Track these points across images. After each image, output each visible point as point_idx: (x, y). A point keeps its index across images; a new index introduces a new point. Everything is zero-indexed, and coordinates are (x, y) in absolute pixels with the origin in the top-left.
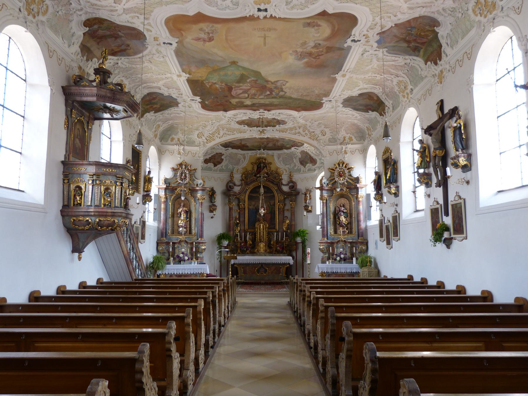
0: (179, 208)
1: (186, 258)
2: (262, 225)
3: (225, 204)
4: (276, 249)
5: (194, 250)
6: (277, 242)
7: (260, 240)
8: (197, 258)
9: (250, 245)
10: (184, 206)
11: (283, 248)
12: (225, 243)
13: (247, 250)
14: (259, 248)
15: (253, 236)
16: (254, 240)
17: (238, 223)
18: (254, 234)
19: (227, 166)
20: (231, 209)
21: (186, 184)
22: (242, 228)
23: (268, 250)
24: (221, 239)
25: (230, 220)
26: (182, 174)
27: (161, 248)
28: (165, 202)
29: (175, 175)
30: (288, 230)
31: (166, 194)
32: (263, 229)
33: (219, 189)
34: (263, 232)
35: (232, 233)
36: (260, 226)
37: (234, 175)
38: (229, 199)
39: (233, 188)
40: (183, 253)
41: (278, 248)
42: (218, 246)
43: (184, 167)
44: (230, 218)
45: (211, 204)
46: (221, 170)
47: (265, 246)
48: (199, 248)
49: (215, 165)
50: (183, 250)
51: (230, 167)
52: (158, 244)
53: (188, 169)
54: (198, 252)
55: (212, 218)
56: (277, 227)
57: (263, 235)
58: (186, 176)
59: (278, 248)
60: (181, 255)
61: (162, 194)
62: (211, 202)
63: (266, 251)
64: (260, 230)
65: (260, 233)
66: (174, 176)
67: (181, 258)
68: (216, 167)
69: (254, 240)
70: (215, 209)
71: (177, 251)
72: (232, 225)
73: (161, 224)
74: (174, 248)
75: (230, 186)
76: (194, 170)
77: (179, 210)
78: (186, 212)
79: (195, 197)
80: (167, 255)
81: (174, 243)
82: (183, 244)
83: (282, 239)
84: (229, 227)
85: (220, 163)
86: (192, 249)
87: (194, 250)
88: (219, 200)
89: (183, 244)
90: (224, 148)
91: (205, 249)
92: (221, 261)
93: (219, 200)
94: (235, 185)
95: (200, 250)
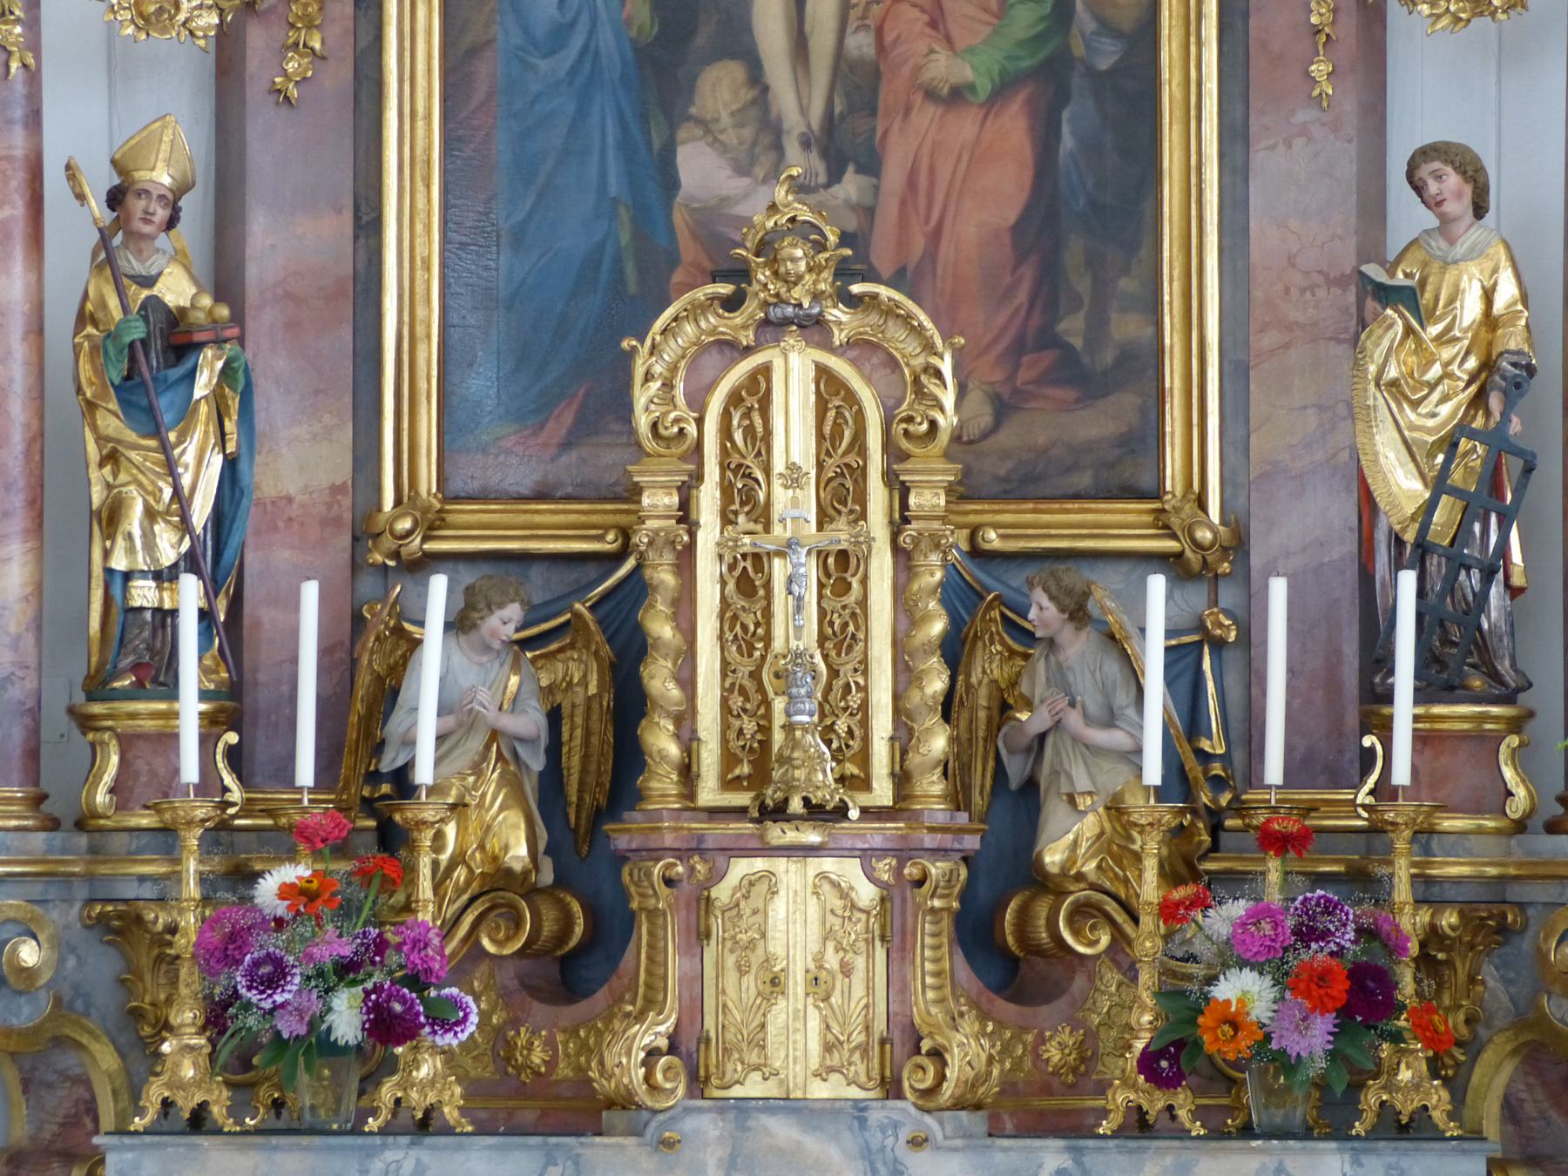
2: (794, 371)
4: (1185, 1002)
6: (1209, 820)
7: (754, 761)
9: (499, 888)
11: (1363, 1000)
13: (387, 1027)
14: (728, 992)
15: (583, 675)
16: (591, 781)
17: (176, 339)
18: (598, 618)
22: (301, 461)
23: (968, 1051)
30: (1487, 499)
32: (840, 495)
34: (841, 567)
36: (755, 396)
41: (1245, 990)
47: (892, 928)
56: (1195, 452)
57: (841, 635)
59: (1245, 990)
63: (900, 1056)
64: (743, 499)
65: (748, 578)
69: (591, 781)
83: (1334, 754)
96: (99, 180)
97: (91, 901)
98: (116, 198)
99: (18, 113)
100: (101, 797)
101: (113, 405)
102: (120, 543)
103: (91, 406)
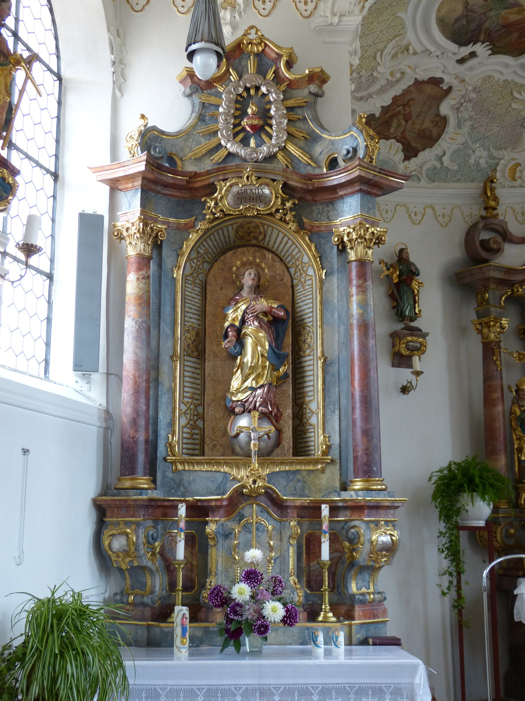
0: (233, 301)
1: (274, 611)
3: (463, 331)
5: (325, 554)
8: (344, 609)
10: (259, 289)
12: (479, 511)
19: (462, 154)
20: (490, 349)
21: (271, 158)
24: (460, 489)
25: (489, 402)
26: (241, 104)
27: (119, 543)
28: (143, 262)
29: (204, 115)
31: (145, 219)
33: (434, 257)
35: (501, 462)
37: (498, 192)
38: (483, 303)
39: (498, 251)
40: (252, 576)
42: (442, 526)
43: (251, 66)
44: (488, 390)
45: (399, 326)
46: (438, 175)
48: (354, 540)
49: (410, 152)
50: (254, 554)
51: (480, 156)
52: (104, 511)
53: (278, 79)
54: (352, 564)
55: (405, 390)
58: (264, 115)
60: (241, 591)
61: (131, 208)
62: (400, 316)
66: (201, 118)
67: (236, 608)
68: (414, 162)
70: (420, 349)
71: (217, 556)
72: (500, 424)
73: (126, 394)
74: (197, 542)
75: (484, 244)
76: (312, 78)
77: (233, 315)
78: (274, 324)
79: (318, 236)
80: (158, 583)
81: (199, 511)
82: (253, 513)
84: (485, 434)
85: (429, 139)
86: (309, 546)
87: (325, 554)
88: (432, 305)
89: (253, 513)
90: (453, 47)
91: (390, 549)
92: (458, 606)
93: (432, 305)
94: (506, 236)
95: (362, 556)
96: (514, 389)
97: (521, 521)
98: (516, 391)
99: (499, 377)
100: (523, 502)
101: (520, 429)
102: (523, 455)
103: (515, 430)
